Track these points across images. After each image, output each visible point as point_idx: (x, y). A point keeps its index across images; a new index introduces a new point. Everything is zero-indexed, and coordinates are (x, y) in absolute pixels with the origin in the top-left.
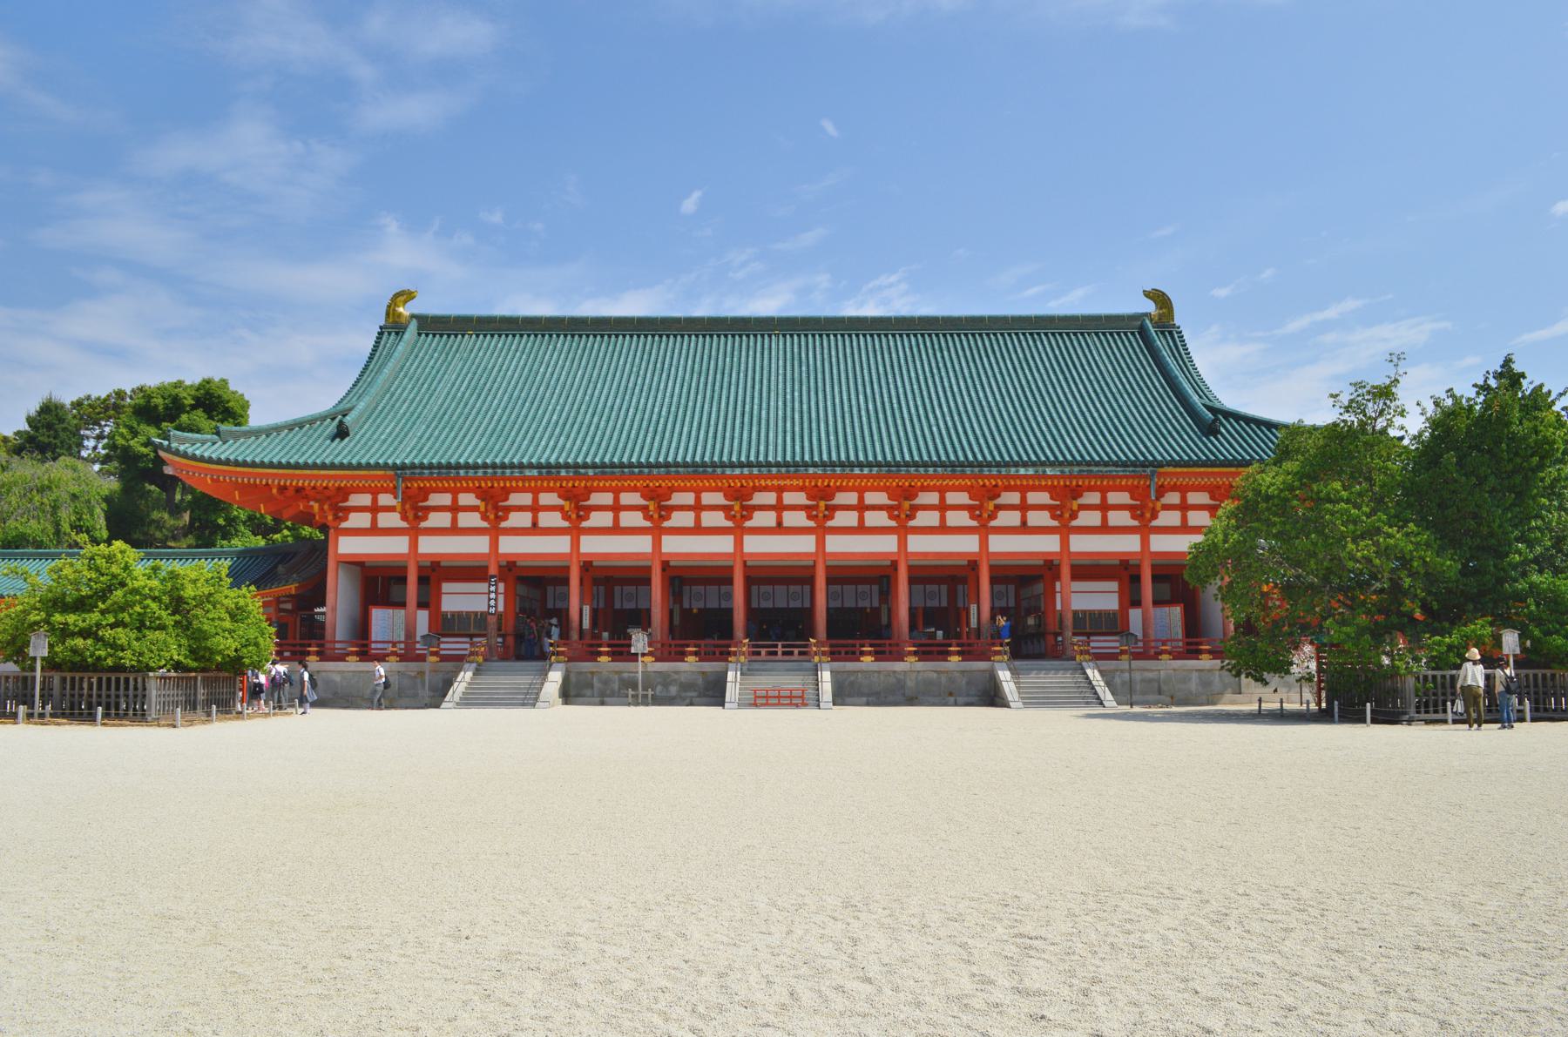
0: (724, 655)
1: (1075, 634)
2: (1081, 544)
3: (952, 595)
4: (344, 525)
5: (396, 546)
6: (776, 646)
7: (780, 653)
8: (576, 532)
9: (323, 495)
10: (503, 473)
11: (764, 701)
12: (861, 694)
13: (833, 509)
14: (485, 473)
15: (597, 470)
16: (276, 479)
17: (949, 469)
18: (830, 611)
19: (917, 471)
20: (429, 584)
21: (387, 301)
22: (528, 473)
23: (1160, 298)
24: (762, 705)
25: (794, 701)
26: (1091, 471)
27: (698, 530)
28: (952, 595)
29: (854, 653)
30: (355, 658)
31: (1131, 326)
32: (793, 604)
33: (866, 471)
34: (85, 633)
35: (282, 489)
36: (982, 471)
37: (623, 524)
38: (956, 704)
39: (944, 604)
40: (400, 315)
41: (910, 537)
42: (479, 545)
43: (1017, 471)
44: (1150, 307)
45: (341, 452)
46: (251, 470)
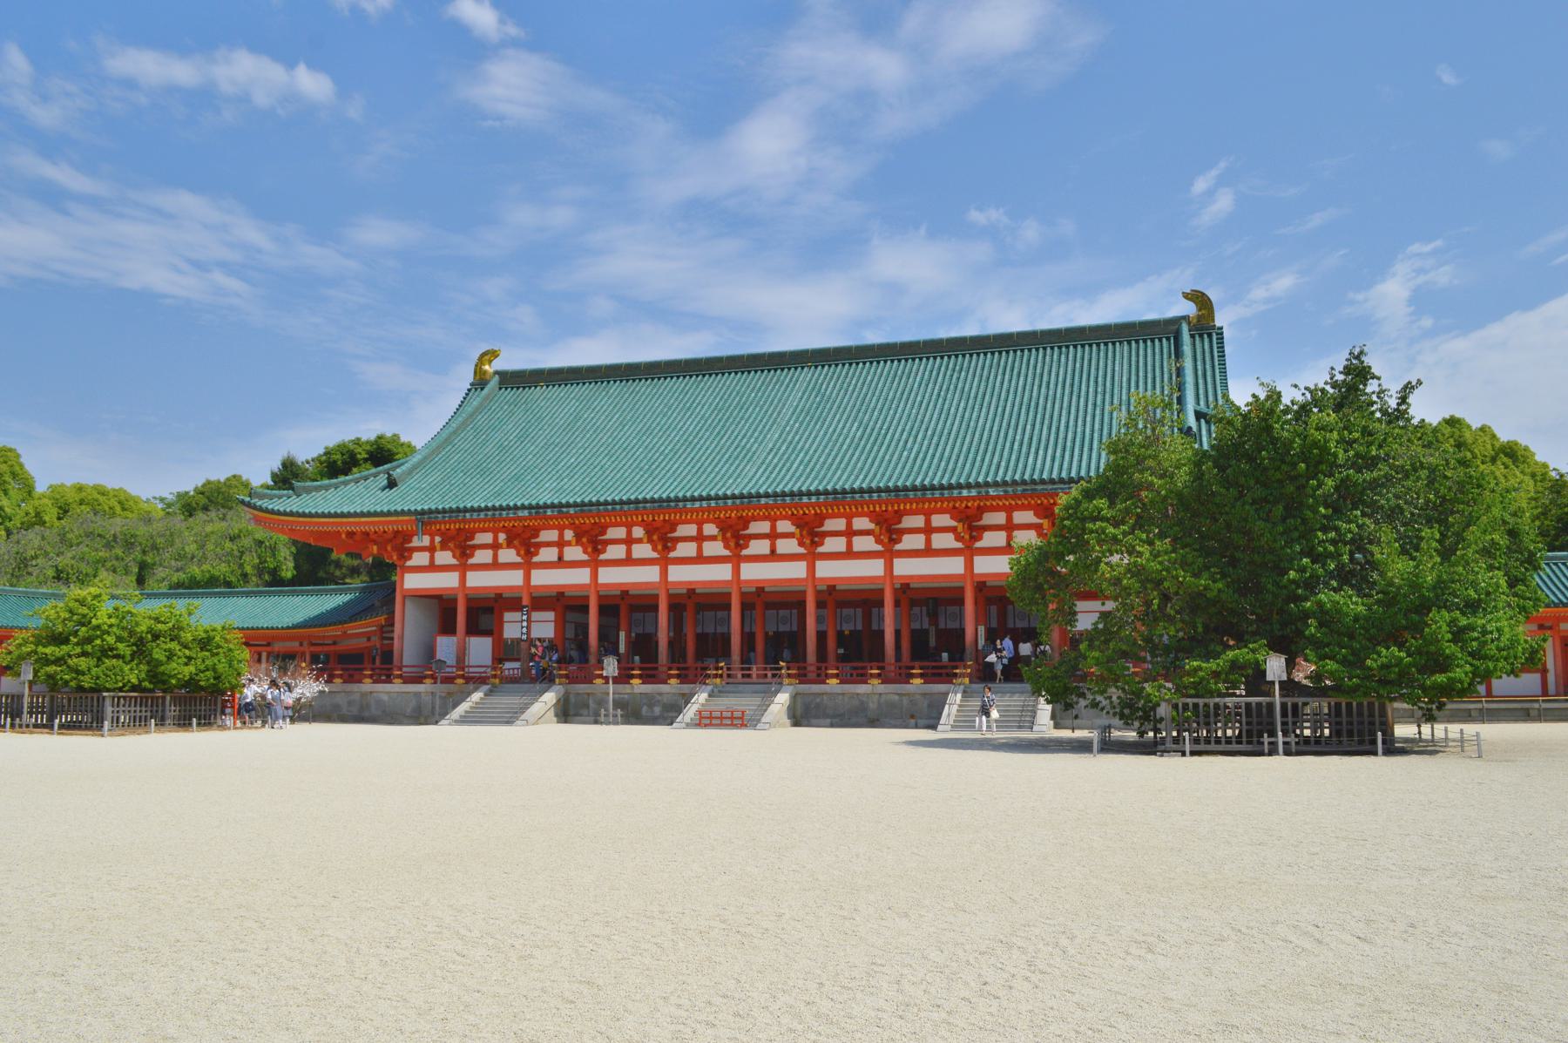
3: (867, 618)
4: (409, 563)
6: (749, 669)
7: (754, 676)
8: (889, 555)
10: (500, 514)
11: (708, 721)
12: (826, 716)
14: (486, 515)
15: (577, 509)
17: (893, 494)
19: (862, 497)
20: (492, 613)
22: (520, 513)
23: (1201, 300)
24: (706, 725)
25: (735, 722)
26: (1035, 490)
28: (867, 618)
29: (862, 675)
30: (400, 681)
31: (1164, 331)
32: (782, 628)
34: (59, 661)
35: (351, 534)
36: (925, 494)
37: (635, 555)
38: (916, 727)
39: (795, 628)
40: (485, 372)
41: (896, 561)
42: (513, 579)
43: (960, 493)
44: (1189, 309)
46: (309, 519)
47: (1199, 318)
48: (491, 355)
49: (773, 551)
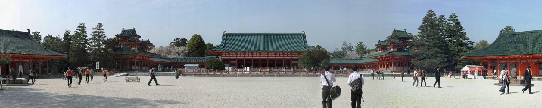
0: (259, 68)
2: (293, 58)
5: (228, 58)
9: (221, 53)
13: (269, 54)
16: (218, 52)
18: (269, 63)
23: (303, 31)
27: (256, 56)
31: (300, 34)
42: (235, 58)
45: (224, 49)
48: (226, 31)
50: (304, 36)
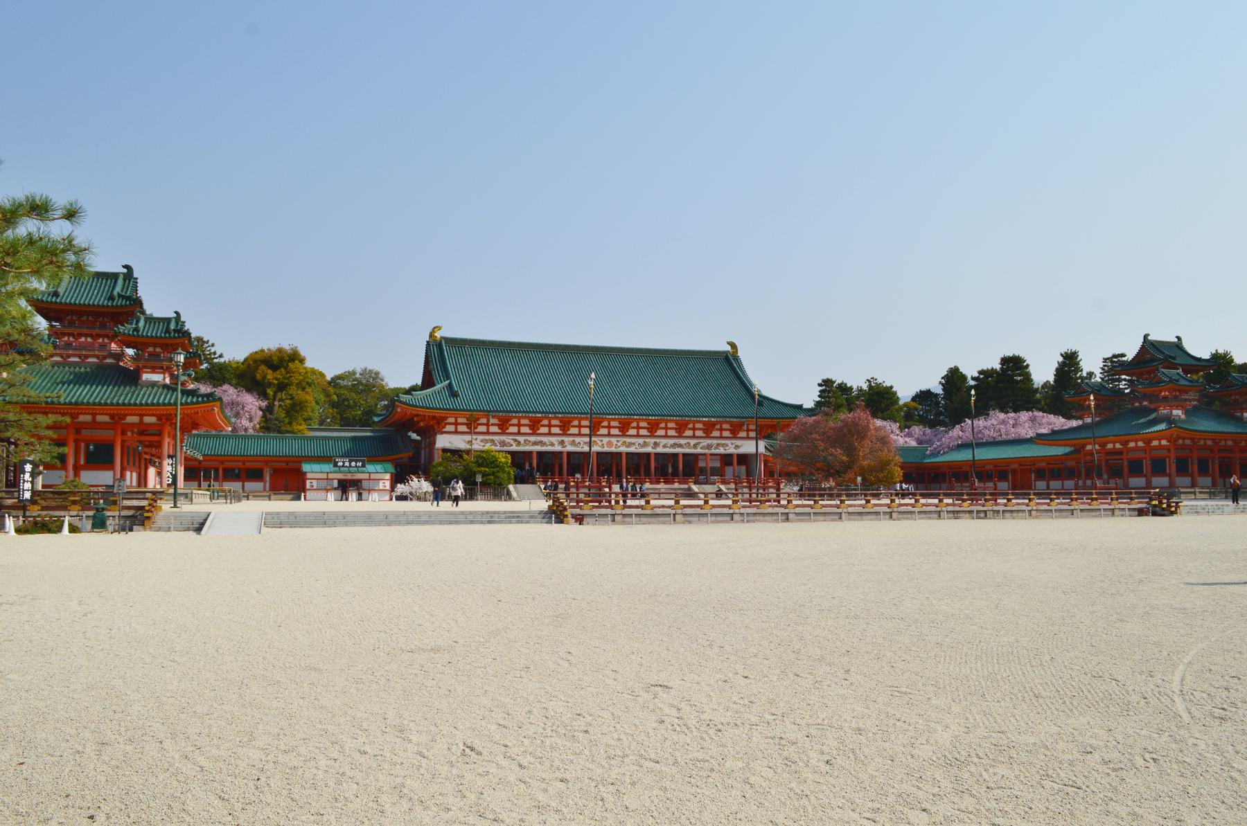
1: (711, 476)
4: (444, 430)
21: (430, 330)
23: (733, 345)
33: (653, 418)
44: (728, 348)
47: (733, 352)
48: (439, 328)
49: (609, 433)
50: (737, 359)
